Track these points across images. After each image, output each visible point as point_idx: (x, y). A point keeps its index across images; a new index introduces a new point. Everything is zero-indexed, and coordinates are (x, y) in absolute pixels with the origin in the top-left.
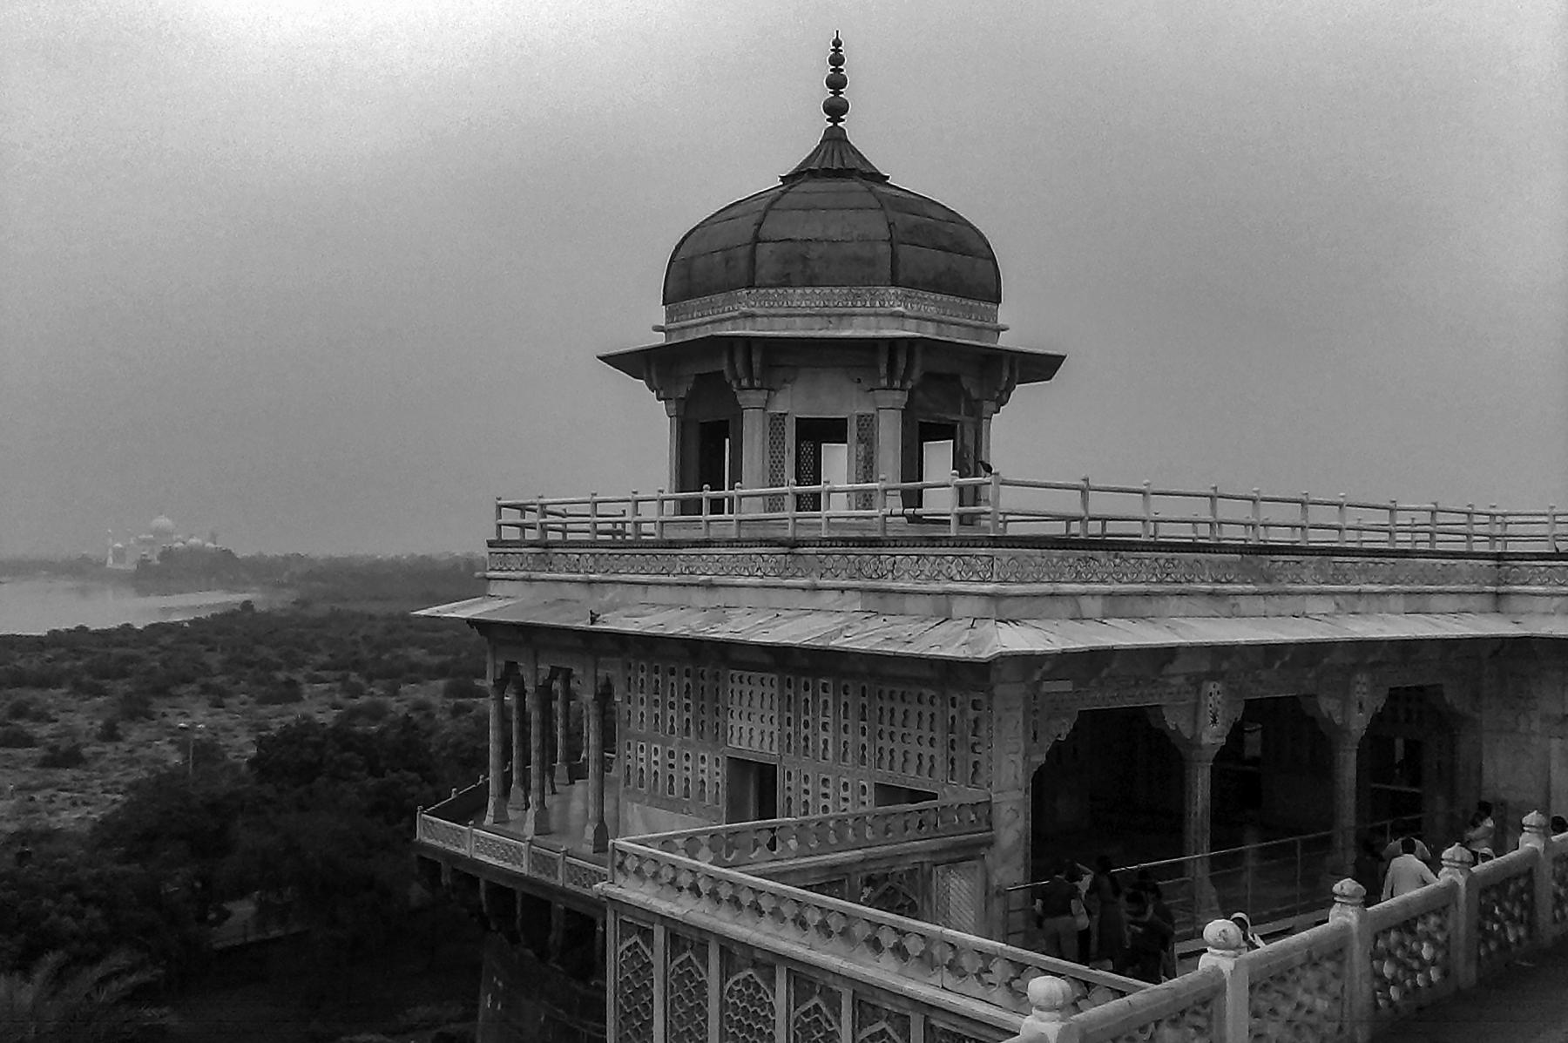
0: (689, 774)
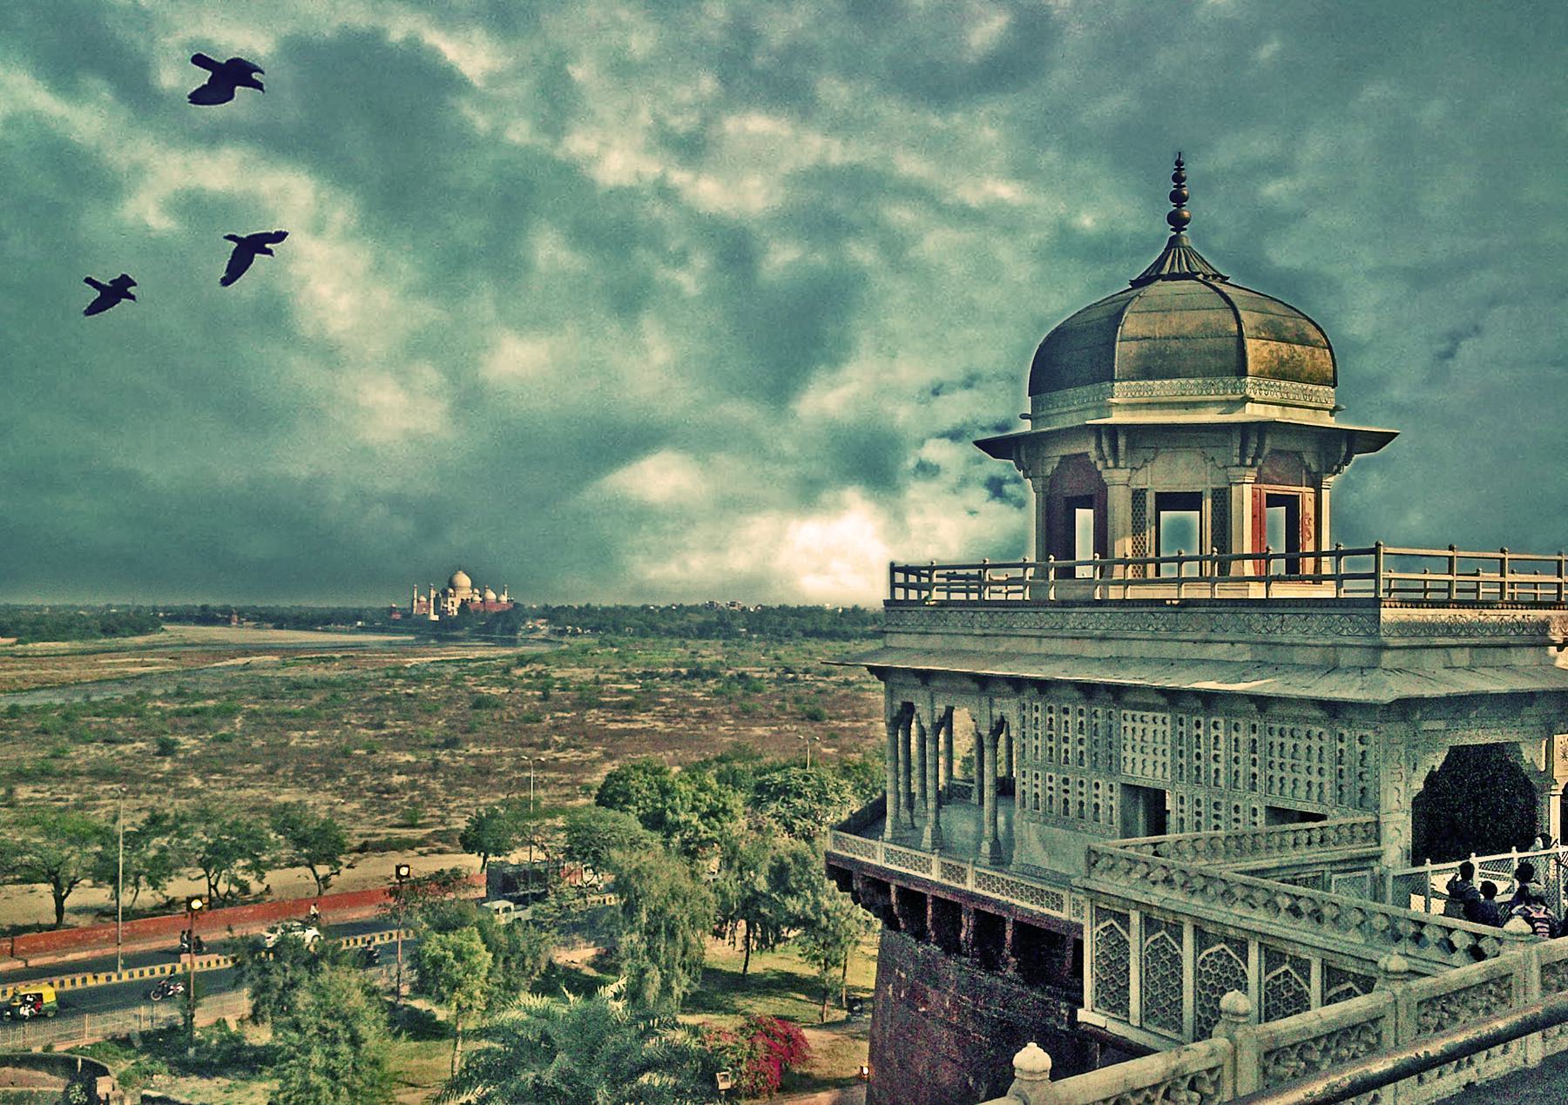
0: (1084, 799)
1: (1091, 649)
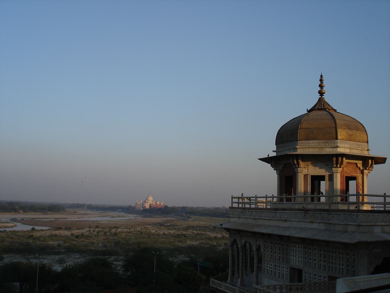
0: (280, 271)
1: (282, 224)
